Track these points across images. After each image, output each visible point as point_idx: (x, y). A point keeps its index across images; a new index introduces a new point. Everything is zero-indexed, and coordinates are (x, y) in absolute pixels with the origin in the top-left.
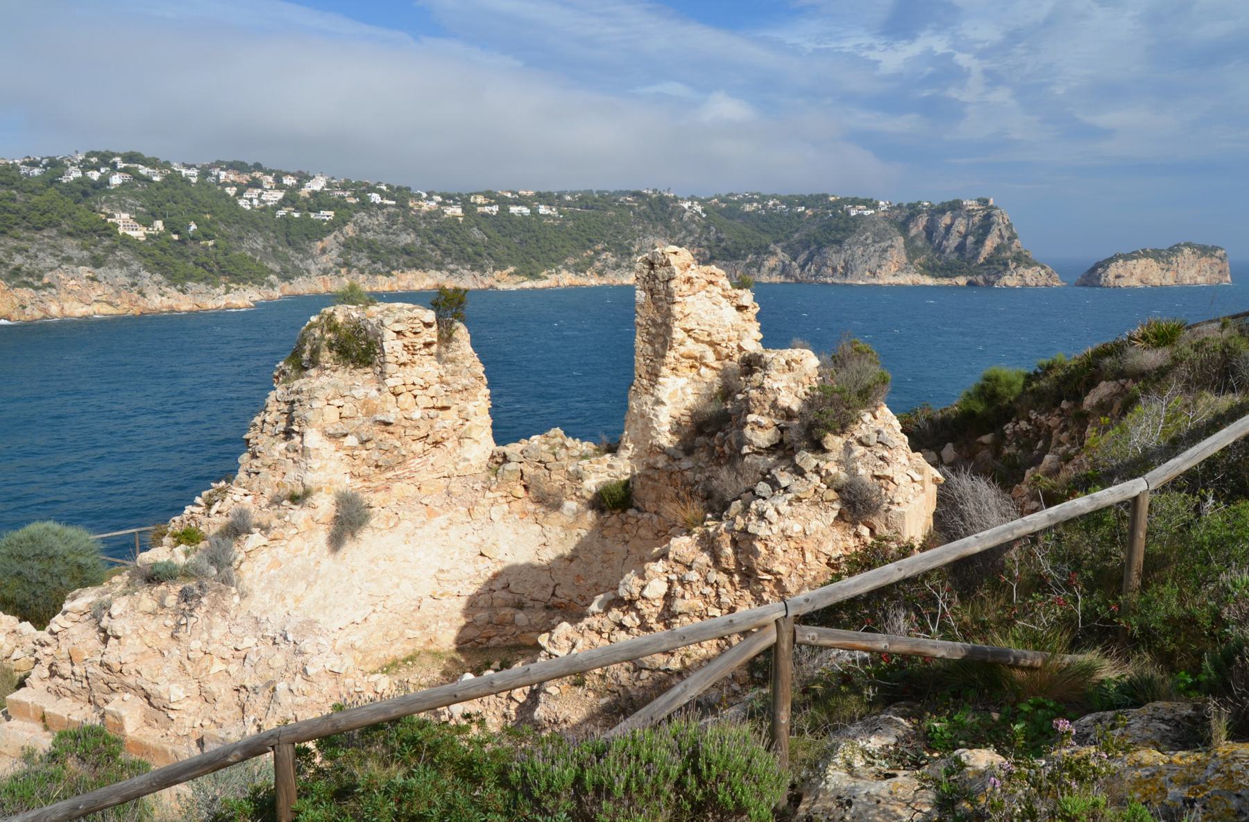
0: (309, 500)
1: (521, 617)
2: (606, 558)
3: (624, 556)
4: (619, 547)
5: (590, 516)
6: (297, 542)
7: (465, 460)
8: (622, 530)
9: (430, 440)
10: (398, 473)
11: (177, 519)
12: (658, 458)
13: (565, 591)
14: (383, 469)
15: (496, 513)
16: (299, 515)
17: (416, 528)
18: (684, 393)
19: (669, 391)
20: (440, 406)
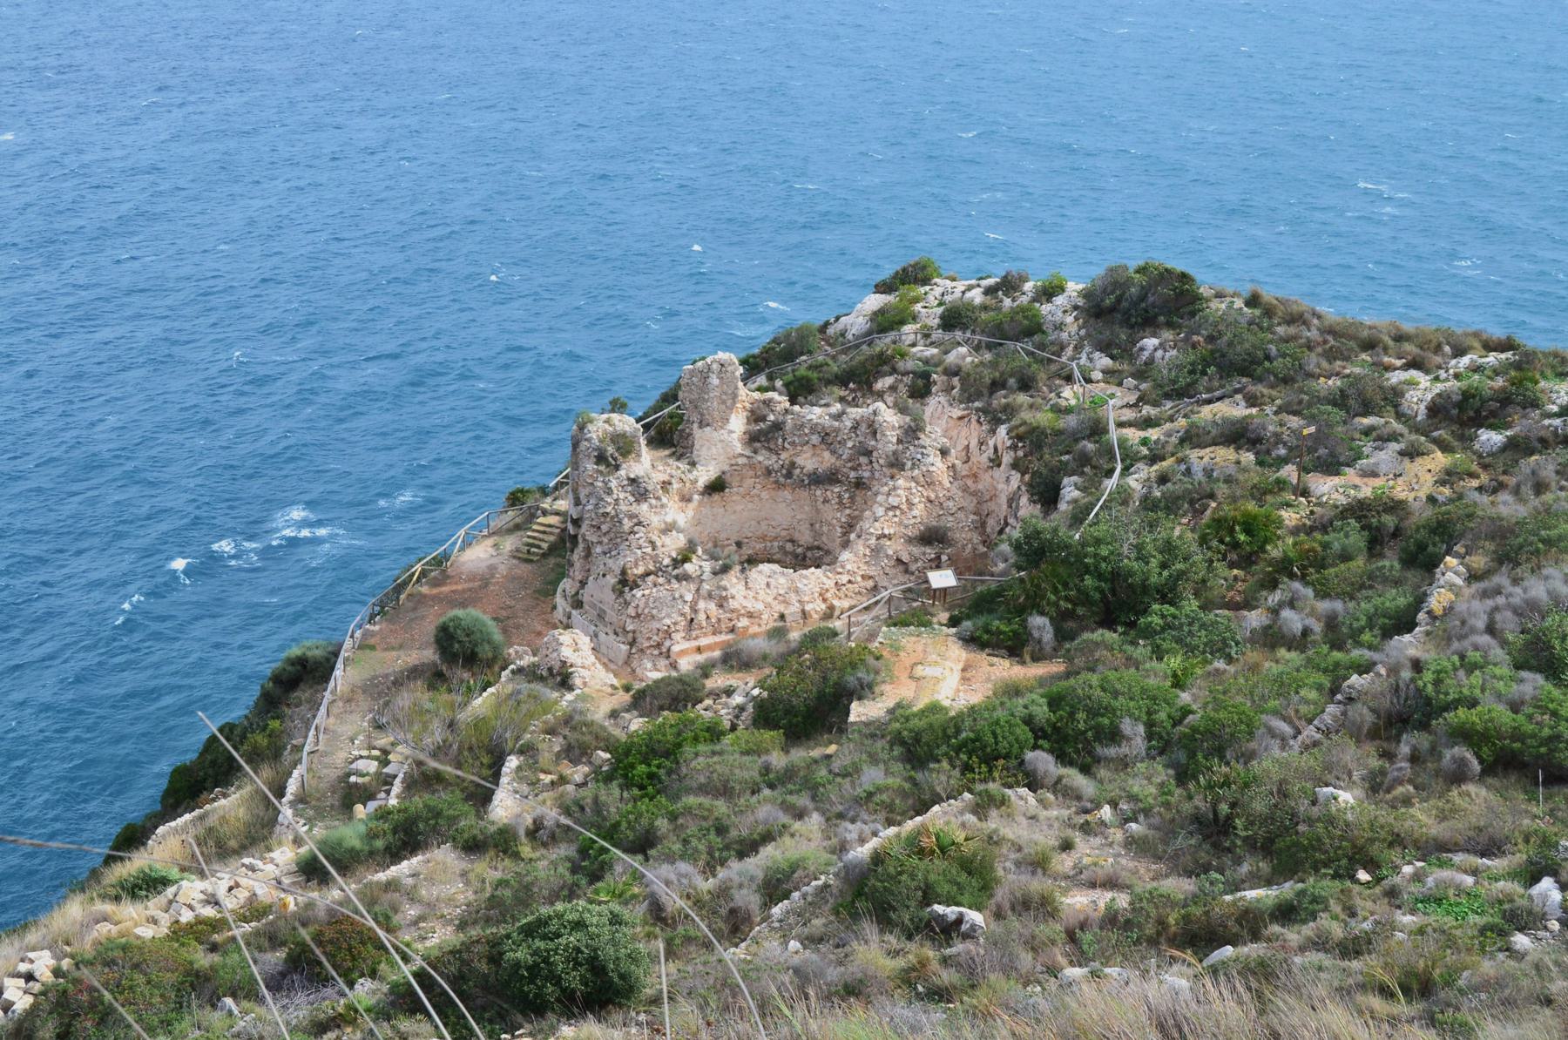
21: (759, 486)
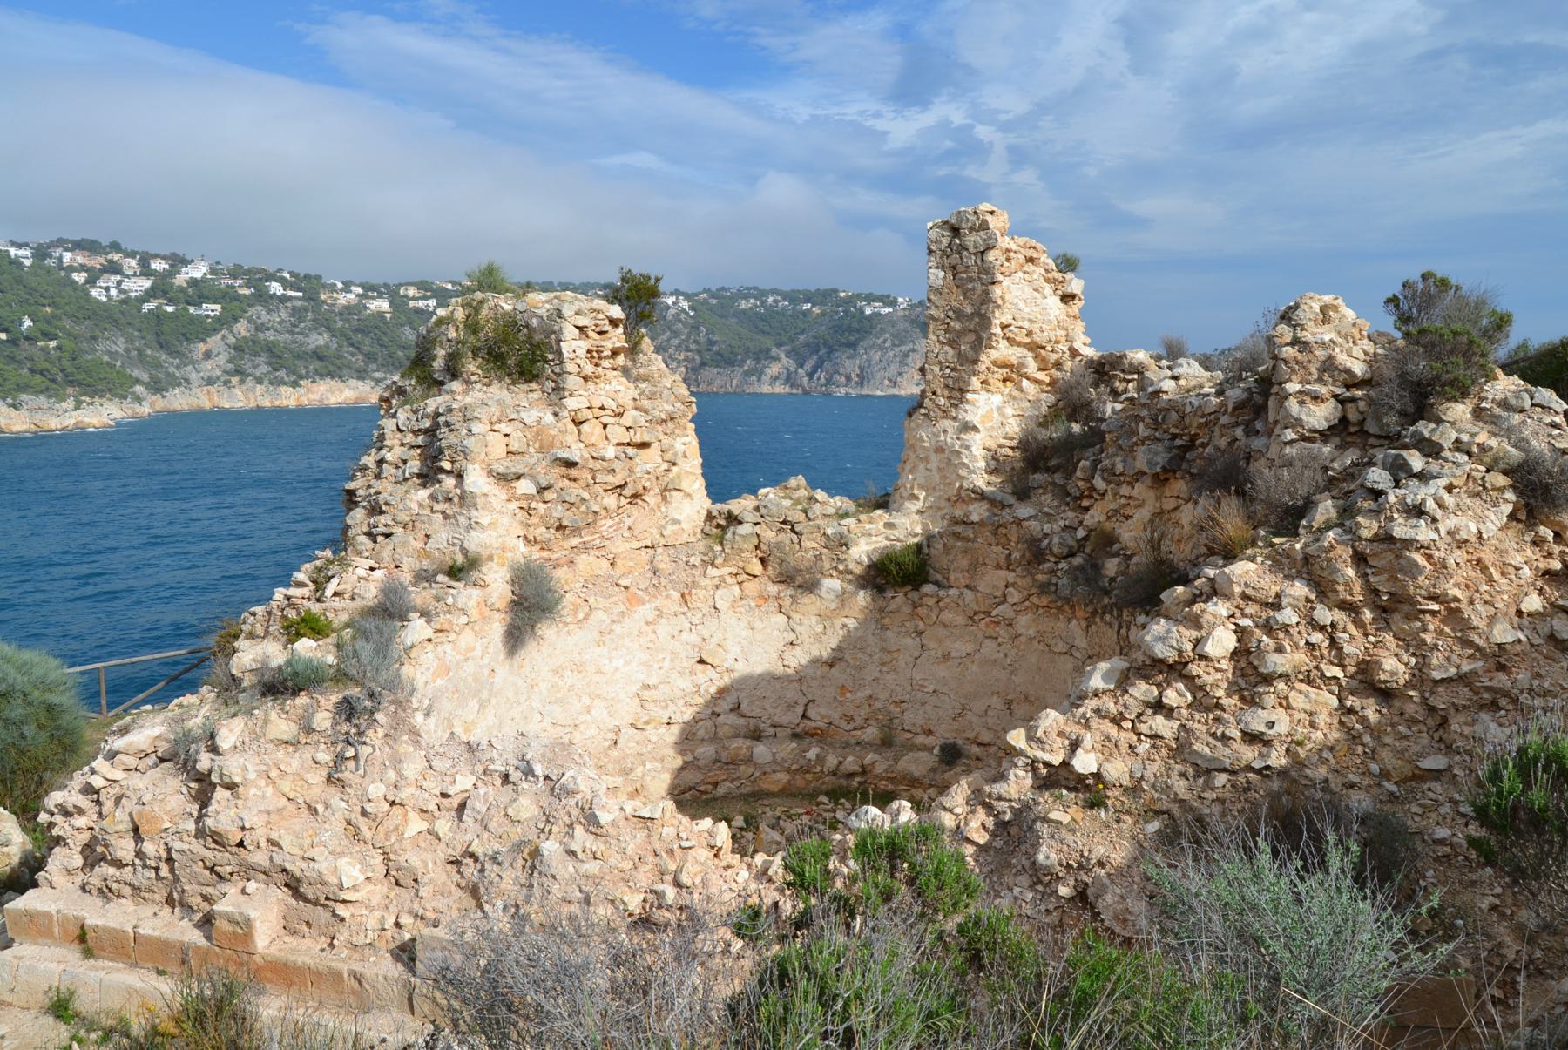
0: (475, 574)
1: (761, 751)
2: (887, 658)
3: (917, 654)
4: (908, 641)
5: (863, 598)
6: (467, 638)
7: (676, 522)
8: (913, 615)
9: (627, 492)
10: (585, 539)
11: (260, 610)
12: (971, 508)
13: (823, 711)
14: (567, 532)
15: (724, 598)
16: (465, 595)
17: (613, 622)
18: (1003, 415)
19: (980, 412)
20: (639, 441)
21: (1015, 596)
